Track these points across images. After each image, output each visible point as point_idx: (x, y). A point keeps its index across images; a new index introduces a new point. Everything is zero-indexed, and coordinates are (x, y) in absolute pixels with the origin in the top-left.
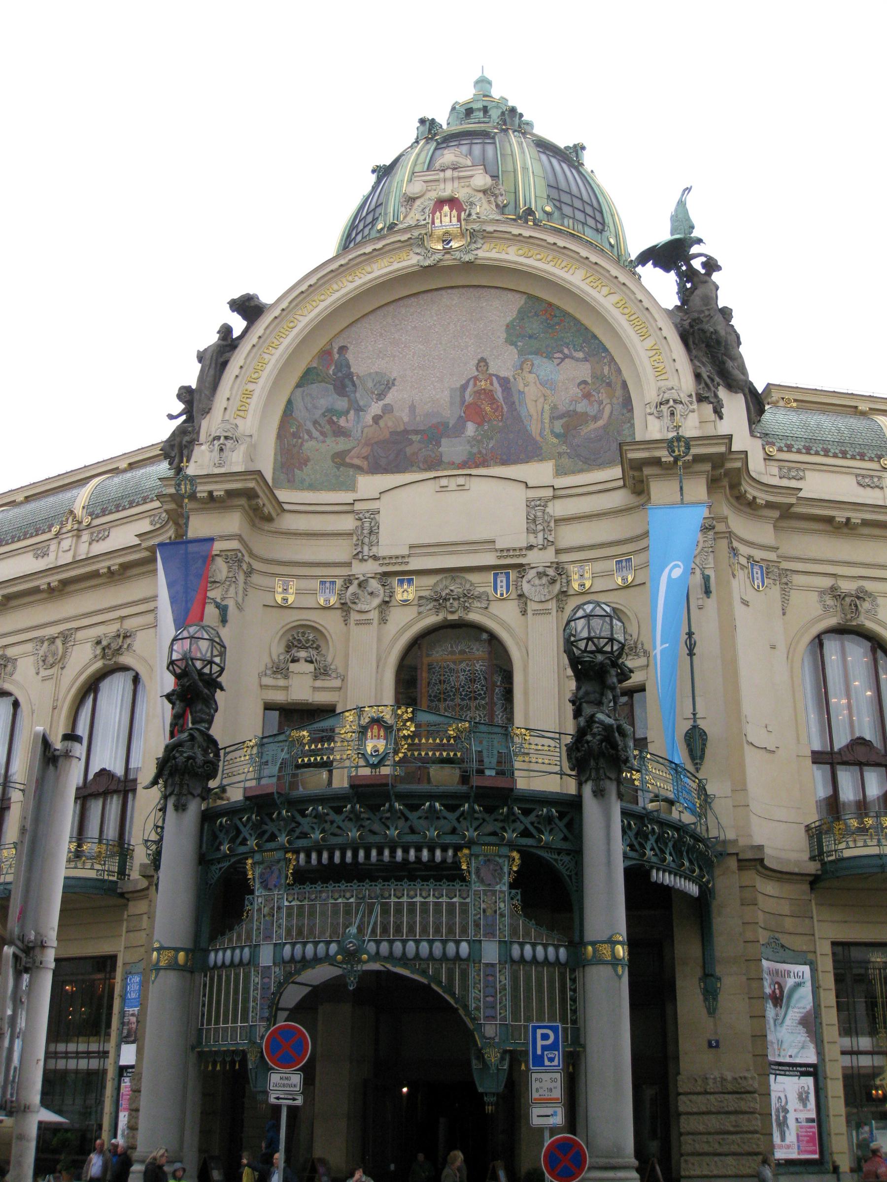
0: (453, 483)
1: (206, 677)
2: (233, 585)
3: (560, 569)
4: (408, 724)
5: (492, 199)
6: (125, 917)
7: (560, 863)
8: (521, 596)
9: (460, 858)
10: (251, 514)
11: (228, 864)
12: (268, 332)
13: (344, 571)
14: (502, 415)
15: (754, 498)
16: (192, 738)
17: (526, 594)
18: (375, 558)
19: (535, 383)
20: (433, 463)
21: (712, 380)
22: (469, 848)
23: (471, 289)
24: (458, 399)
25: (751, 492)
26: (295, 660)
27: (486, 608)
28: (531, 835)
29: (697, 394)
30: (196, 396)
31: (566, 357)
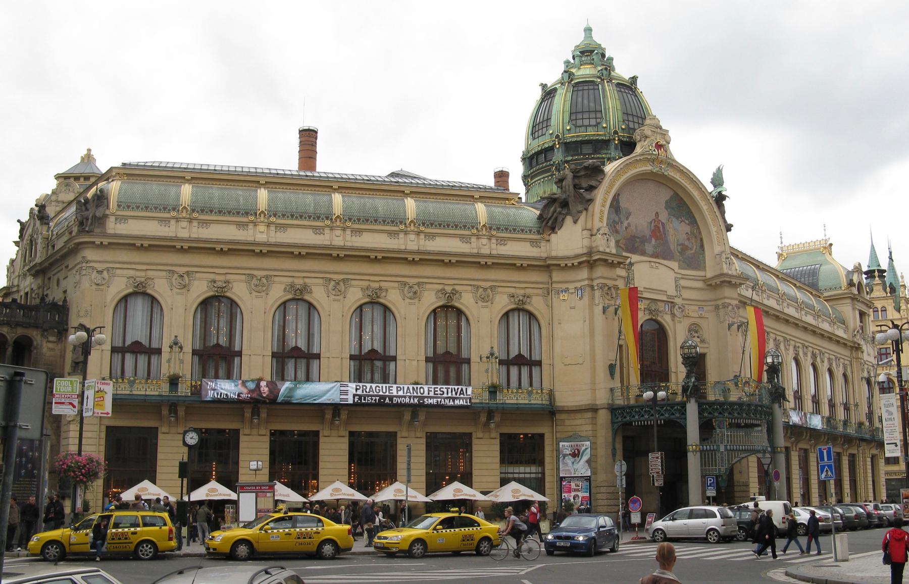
20: (643, 253)
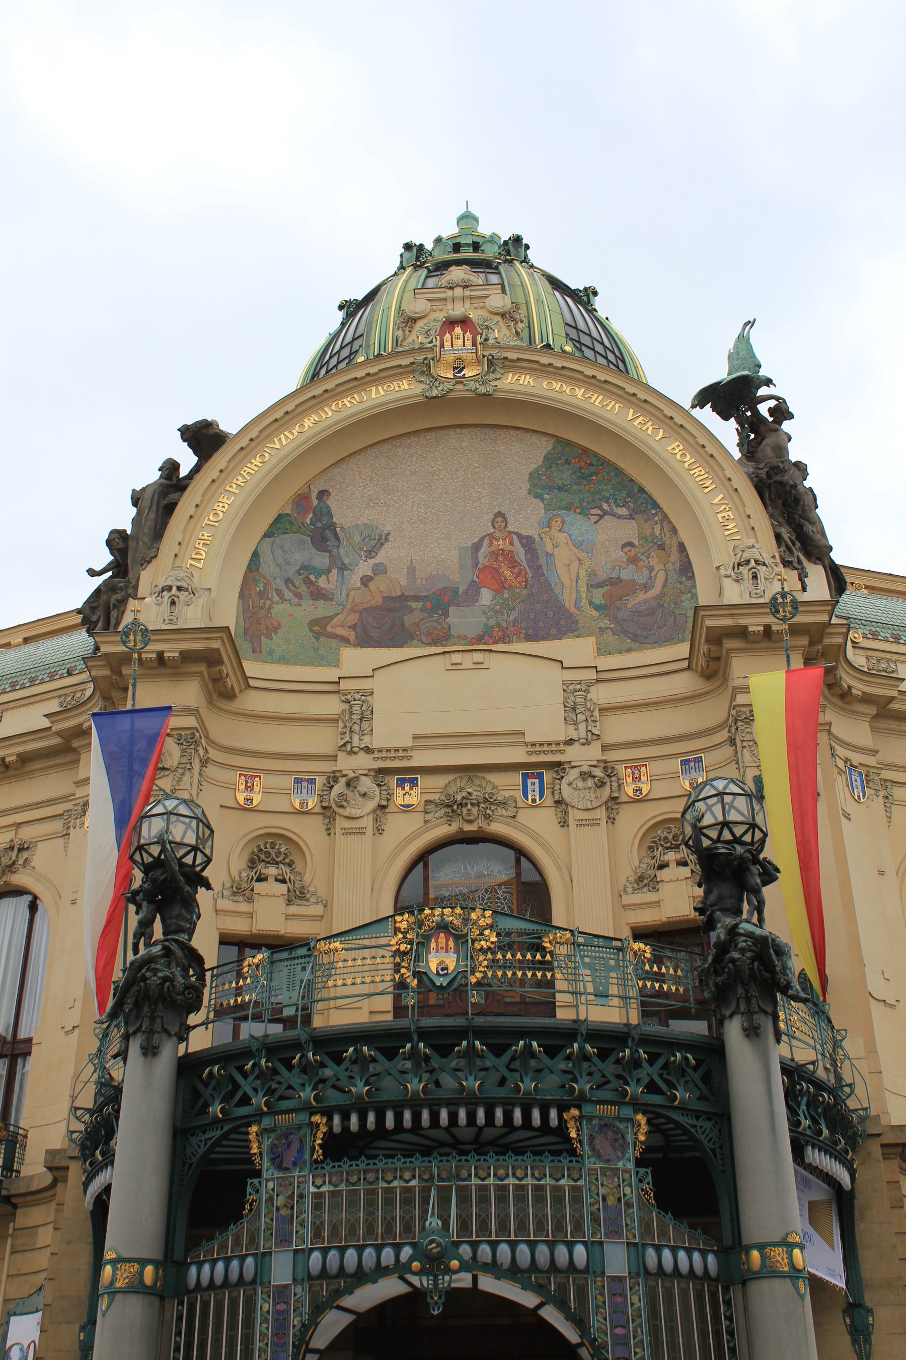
0: (467, 660)
1: (188, 869)
2: (188, 774)
3: (609, 769)
4: (487, 932)
5: (512, 324)
6: (11, 1231)
7: (700, 1131)
8: (557, 802)
9: (566, 1121)
10: (211, 686)
11: (219, 1133)
12: (232, 465)
13: (327, 767)
14: (526, 582)
15: (850, 687)
16: (167, 952)
17: (568, 800)
18: (368, 750)
19: (567, 544)
20: (440, 637)
21: (794, 544)
22: (579, 1107)
23: (486, 430)
24: (469, 561)
25: (847, 679)
26: (261, 879)
27: (514, 817)
28: (660, 1092)
29: (781, 556)
30: (132, 544)
31: (606, 513)
